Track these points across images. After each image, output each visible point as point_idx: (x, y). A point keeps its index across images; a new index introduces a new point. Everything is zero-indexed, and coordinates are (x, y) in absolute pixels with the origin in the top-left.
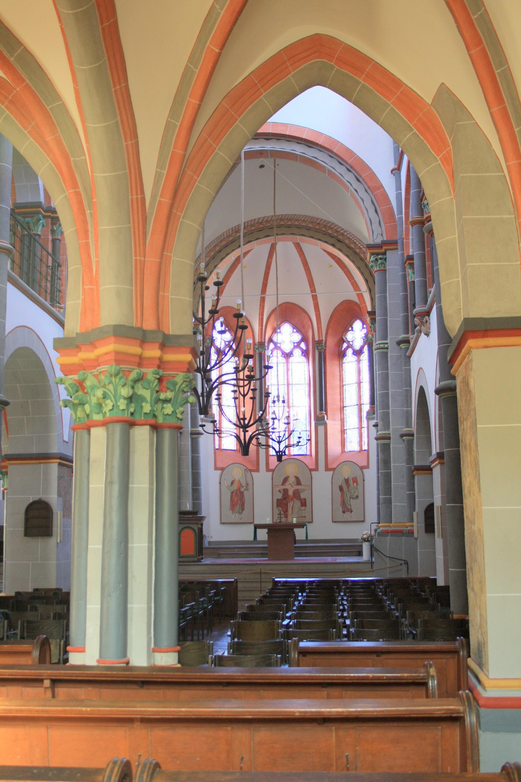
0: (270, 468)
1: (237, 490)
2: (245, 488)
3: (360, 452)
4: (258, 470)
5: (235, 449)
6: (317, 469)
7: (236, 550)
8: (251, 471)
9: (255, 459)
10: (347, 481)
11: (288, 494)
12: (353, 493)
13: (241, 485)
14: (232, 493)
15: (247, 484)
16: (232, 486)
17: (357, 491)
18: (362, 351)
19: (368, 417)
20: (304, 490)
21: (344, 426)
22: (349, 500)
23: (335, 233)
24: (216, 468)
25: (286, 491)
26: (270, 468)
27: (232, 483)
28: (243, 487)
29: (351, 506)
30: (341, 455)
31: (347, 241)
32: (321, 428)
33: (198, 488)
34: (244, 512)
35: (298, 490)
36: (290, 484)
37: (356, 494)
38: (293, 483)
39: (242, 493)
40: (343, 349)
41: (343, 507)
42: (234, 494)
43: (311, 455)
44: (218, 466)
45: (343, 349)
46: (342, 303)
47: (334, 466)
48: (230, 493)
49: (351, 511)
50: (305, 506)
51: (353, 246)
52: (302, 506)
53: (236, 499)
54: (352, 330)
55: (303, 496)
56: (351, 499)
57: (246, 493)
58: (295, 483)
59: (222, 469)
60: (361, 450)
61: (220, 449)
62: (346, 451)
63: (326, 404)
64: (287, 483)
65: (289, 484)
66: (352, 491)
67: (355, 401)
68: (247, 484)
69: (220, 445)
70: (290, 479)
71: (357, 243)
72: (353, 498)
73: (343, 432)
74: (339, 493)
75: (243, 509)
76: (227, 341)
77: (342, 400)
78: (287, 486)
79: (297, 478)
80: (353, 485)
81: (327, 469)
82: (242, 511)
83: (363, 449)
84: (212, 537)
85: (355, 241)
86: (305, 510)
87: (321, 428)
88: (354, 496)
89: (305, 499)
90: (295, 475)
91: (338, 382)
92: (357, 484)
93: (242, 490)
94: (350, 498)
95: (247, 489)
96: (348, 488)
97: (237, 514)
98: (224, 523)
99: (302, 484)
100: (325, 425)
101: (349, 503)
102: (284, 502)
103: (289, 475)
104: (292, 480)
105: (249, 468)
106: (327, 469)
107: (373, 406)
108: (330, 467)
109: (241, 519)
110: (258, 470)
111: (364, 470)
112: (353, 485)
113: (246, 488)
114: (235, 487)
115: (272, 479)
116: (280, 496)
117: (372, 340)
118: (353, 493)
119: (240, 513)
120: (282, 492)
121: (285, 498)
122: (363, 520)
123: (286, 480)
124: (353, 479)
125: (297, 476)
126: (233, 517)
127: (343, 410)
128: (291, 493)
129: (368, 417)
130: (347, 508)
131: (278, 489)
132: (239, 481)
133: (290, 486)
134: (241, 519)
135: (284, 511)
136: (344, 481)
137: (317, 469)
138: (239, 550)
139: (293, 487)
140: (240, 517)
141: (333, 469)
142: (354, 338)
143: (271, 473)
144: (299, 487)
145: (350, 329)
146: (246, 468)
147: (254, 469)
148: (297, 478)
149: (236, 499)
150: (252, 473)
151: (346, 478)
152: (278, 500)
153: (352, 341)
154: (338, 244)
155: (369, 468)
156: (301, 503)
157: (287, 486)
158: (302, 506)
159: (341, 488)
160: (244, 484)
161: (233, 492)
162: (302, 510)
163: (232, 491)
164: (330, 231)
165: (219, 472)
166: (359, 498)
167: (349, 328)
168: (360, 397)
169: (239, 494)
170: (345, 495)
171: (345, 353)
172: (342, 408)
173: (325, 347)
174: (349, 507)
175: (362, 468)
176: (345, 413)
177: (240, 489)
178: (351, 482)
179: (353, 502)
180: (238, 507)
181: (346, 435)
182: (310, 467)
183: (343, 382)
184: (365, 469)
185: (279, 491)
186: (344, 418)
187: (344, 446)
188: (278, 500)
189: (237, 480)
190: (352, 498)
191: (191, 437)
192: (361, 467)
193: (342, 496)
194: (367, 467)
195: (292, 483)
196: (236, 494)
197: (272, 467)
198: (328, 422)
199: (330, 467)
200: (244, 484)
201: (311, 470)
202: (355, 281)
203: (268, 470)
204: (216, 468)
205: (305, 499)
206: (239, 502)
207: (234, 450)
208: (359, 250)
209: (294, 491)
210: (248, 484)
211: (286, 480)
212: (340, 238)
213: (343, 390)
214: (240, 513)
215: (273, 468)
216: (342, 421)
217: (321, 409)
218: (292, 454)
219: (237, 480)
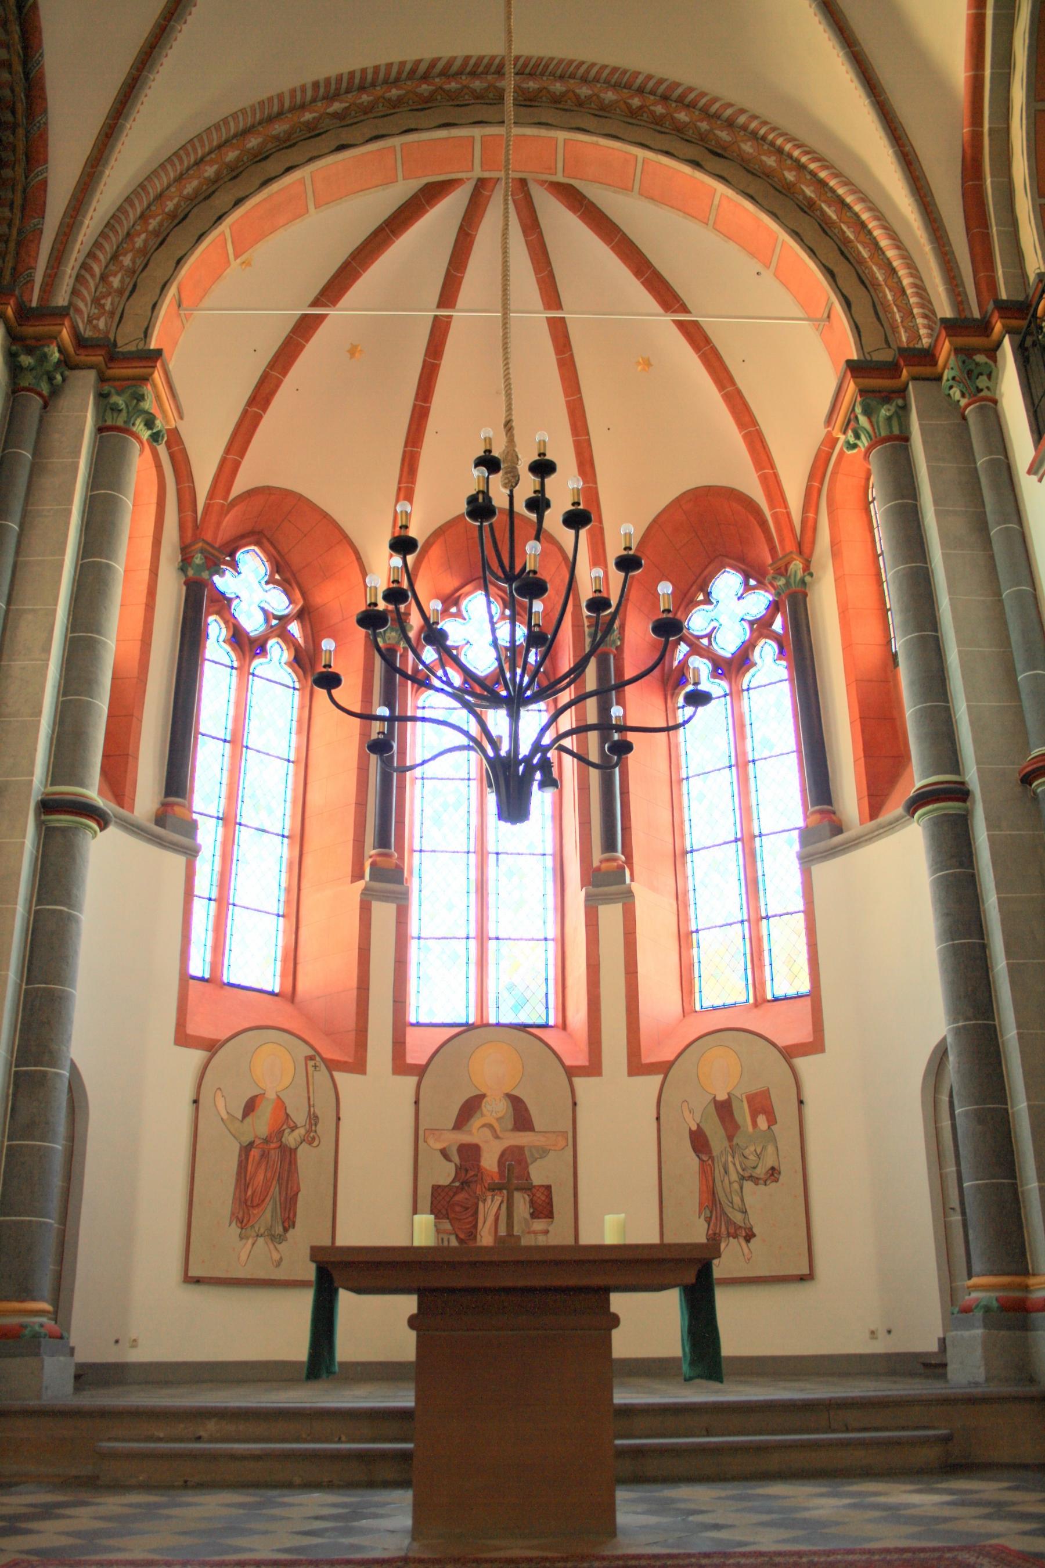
0: (410, 1059)
1: (267, 1141)
2: (302, 1131)
3: (756, 1005)
4: (358, 1066)
5: (277, 990)
6: (594, 1068)
7: (211, 1426)
8: (332, 1065)
9: (351, 1022)
10: (724, 1109)
11: (479, 1167)
12: (752, 1157)
13: (283, 1120)
14: (246, 1150)
15: (313, 1119)
16: (248, 1120)
17: (770, 1149)
18: (747, 658)
19: (810, 849)
20: (544, 1152)
21: (687, 920)
22: (736, 1186)
23: (702, 121)
24: (183, 1038)
25: (470, 1153)
26: (410, 1059)
27: (250, 1107)
28: (294, 1128)
29: (745, 1212)
30: (681, 1021)
31: (748, 147)
32: (611, 915)
33: (44, 1074)
34: (291, 1232)
35: (520, 1149)
36: (489, 1126)
37: (769, 1161)
38: (498, 1119)
39: (289, 1155)
40: (676, 663)
41: (708, 1220)
42: (255, 1153)
43: (564, 1026)
44: (192, 1029)
45: (676, 663)
46: (677, 502)
47: (668, 1055)
48: (236, 1148)
49: (749, 1237)
50: (550, 1215)
51: (771, 161)
52: (533, 1216)
53: (260, 1177)
54: (708, 601)
55: (538, 1175)
56: (748, 1185)
57: (305, 1156)
58: (510, 1126)
59: (212, 1047)
60: (760, 1001)
61: (214, 981)
62: (698, 1008)
63: (626, 829)
64: (476, 1122)
65: (484, 1126)
66: (749, 1151)
67: (728, 827)
68: (313, 1119)
69: (217, 964)
70: (487, 1106)
71: (788, 147)
72: (756, 1180)
73: (685, 938)
74: (692, 1161)
75: (289, 1222)
76: (276, 617)
77: (677, 828)
78: (475, 1133)
79: (516, 1102)
80: (755, 1124)
81: (637, 1067)
82: (286, 1230)
83: (769, 997)
84: (134, 1343)
85: (779, 142)
86: (546, 1232)
87: (611, 915)
88: (760, 1171)
89: (548, 1188)
90: (507, 1090)
91: (663, 765)
92: (772, 1121)
93: (291, 1139)
94: (743, 1178)
95: (310, 1139)
96: (730, 1138)
97: (261, 1240)
98: (198, 1281)
99: (537, 1128)
100: (627, 898)
101: (736, 1199)
102: (461, 1197)
103: (484, 1090)
104: (496, 1109)
105: (327, 1055)
106: (637, 1067)
107: (825, 807)
108: (647, 1058)
109: (278, 1264)
110: (358, 1066)
111: (800, 1062)
112: (755, 1124)
113: (308, 1132)
114: (261, 1124)
115: (417, 1103)
116: (444, 1173)
117: (803, 582)
118: (752, 1157)
119: (277, 1239)
120: (456, 1159)
121: (465, 1184)
122: (806, 1271)
123: (470, 1108)
124: (751, 1099)
125: (515, 1093)
126: (244, 1257)
127: (684, 863)
128: (489, 1161)
129: (810, 849)
130: (730, 1222)
131: (440, 1146)
132: (280, 1104)
133: (487, 1132)
134: (278, 1264)
135: (462, 1236)
136: (712, 1109)
137: (594, 1068)
138: (230, 1428)
139: (497, 1137)
140: (276, 1256)
141: (664, 1068)
142: (714, 624)
143: (412, 1080)
144: (523, 1139)
145: (701, 597)
146: (311, 1053)
147: (346, 1059)
148: (516, 1102)
149: (260, 1177)
150: (339, 1076)
151: (722, 1097)
152: (436, 1189)
153: (709, 636)
154: (712, 162)
155: (822, 1050)
156: (532, 1203)
157: (475, 1133)
158: (533, 1216)
159: (699, 1141)
160: (299, 1117)
161: (251, 1144)
162: (535, 1233)
163: (246, 1140)
164: (682, 116)
165: (195, 1057)
166: (782, 1179)
167: (695, 595)
168: (746, 811)
169: (274, 1155)
170: (718, 1171)
171: (683, 675)
172: (679, 856)
173: (622, 639)
174: (737, 1218)
175: (789, 1053)
176: (689, 873)
177: (281, 1133)
178: (742, 1113)
179: (754, 1196)
180: (268, 1214)
181: (695, 950)
182: (568, 1062)
183: (679, 768)
184: (805, 1054)
185: (444, 1153)
186: (686, 892)
187: (691, 992)
188: (436, 1189)
189: (271, 1095)
190: (751, 1178)
191: (40, 824)
192: (786, 1048)
193: (706, 1173)
194: (816, 1045)
195: (496, 1125)
196: (264, 1155)
197: (417, 1052)
198: (635, 887)
199: (647, 1058)
200: (299, 1117)
201: (571, 1072)
202: (739, 392)
203: (401, 1066)
204: (183, 1038)
205: (548, 1188)
206: (275, 1189)
207: (272, 993)
208: (794, 173)
209: (502, 1155)
210: (317, 1117)
211: (470, 1108)
212: (718, 139)
213: (680, 795)
214: (277, 1239)
215: (423, 1061)
216: (681, 900)
217: (609, 845)
218: (492, 1020)
219: (271, 1095)
